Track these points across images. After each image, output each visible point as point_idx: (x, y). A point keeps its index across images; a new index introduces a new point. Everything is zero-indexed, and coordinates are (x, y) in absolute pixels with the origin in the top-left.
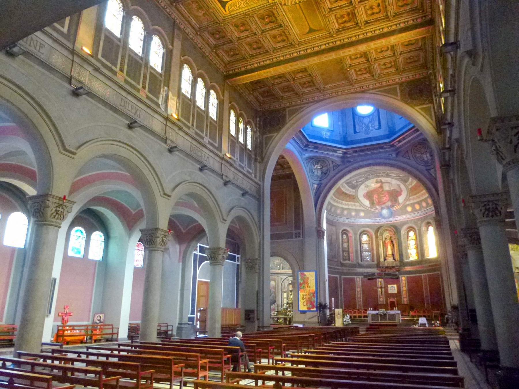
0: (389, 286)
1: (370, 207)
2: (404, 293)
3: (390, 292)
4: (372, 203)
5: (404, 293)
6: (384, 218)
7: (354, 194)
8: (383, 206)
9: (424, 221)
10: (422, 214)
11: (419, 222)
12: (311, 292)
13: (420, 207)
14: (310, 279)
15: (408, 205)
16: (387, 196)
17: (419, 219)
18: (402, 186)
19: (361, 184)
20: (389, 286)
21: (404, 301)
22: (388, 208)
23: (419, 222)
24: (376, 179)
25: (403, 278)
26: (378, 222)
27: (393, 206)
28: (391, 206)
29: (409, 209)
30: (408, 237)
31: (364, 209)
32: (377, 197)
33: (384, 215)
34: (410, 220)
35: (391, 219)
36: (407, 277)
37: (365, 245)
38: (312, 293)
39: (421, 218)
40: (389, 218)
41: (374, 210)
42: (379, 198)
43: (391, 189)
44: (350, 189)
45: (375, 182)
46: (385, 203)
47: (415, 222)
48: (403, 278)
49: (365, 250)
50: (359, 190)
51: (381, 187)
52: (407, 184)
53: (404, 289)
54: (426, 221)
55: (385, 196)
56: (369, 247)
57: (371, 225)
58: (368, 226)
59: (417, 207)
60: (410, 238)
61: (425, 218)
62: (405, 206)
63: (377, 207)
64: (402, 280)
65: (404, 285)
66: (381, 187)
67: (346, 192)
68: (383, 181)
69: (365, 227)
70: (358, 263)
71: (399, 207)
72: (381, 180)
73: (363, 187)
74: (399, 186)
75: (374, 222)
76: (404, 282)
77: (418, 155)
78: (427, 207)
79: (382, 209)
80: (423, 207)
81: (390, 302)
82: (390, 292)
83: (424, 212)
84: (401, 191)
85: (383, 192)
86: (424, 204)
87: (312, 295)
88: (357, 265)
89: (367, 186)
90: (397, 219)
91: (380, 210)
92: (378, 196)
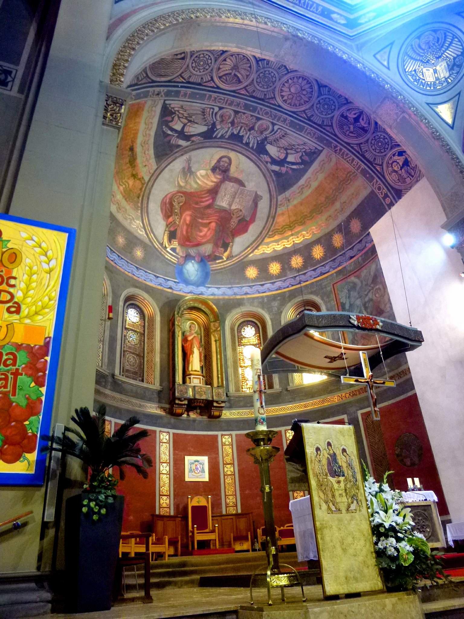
0: (188, 459)
1: (162, 244)
2: (229, 480)
3: (189, 477)
4: (172, 236)
5: (229, 480)
6: (187, 282)
7: (146, 179)
8: (192, 252)
9: (290, 301)
10: (287, 283)
11: (275, 304)
12: (18, 338)
13: (283, 269)
14: (27, 260)
15: (253, 263)
16: (213, 225)
17: (274, 298)
18: (263, 206)
19: (186, 151)
20: (188, 459)
21: (227, 506)
22: (203, 260)
23: (275, 304)
24: (222, 152)
25: (227, 440)
26: (170, 288)
27: (213, 258)
28: (209, 256)
29: (252, 272)
30: (241, 338)
31: (147, 241)
32: (188, 218)
33: (186, 275)
34: (249, 299)
35: (202, 289)
36: (236, 435)
37: (130, 333)
38: (29, 349)
39: (282, 295)
40: (198, 284)
41: (168, 256)
42: (193, 225)
43: (234, 207)
44: (152, 152)
45: (213, 163)
46: (198, 245)
47: (265, 303)
48: (227, 440)
49: (130, 348)
50: (166, 174)
51: (214, 192)
52: (280, 198)
53: (229, 469)
54: (299, 299)
55: (207, 225)
56: (142, 342)
57: (152, 289)
58: (148, 290)
59: (275, 268)
60: (244, 341)
61: (292, 295)
62: (243, 265)
63: (178, 249)
64: (223, 444)
65: (228, 459)
66: (214, 192)
67: (138, 150)
68: (233, 172)
69: (139, 288)
70: (113, 376)
71: (229, 263)
72: (230, 164)
73: (178, 164)
74: (256, 199)
75: (160, 285)
76: (228, 449)
77: (410, 67)
78: (305, 266)
79: (188, 257)
80: (291, 269)
81: (193, 507)
82: (189, 477)
83: (292, 281)
84: (253, 219)
85: (209, 211)
86: (297, 261)
87: (22, 358)
88: (110, 379)
89: (188, 171)
90: (216, 291)
91: (181, 260)
92: (194, 219)
